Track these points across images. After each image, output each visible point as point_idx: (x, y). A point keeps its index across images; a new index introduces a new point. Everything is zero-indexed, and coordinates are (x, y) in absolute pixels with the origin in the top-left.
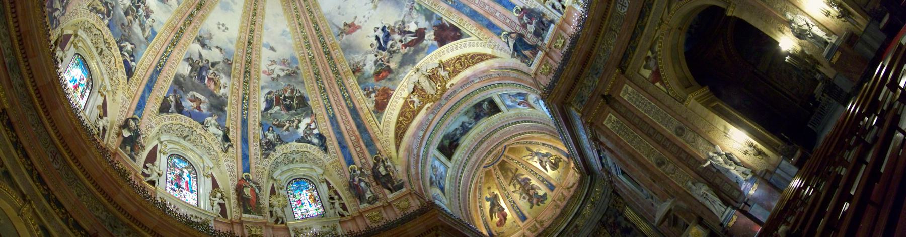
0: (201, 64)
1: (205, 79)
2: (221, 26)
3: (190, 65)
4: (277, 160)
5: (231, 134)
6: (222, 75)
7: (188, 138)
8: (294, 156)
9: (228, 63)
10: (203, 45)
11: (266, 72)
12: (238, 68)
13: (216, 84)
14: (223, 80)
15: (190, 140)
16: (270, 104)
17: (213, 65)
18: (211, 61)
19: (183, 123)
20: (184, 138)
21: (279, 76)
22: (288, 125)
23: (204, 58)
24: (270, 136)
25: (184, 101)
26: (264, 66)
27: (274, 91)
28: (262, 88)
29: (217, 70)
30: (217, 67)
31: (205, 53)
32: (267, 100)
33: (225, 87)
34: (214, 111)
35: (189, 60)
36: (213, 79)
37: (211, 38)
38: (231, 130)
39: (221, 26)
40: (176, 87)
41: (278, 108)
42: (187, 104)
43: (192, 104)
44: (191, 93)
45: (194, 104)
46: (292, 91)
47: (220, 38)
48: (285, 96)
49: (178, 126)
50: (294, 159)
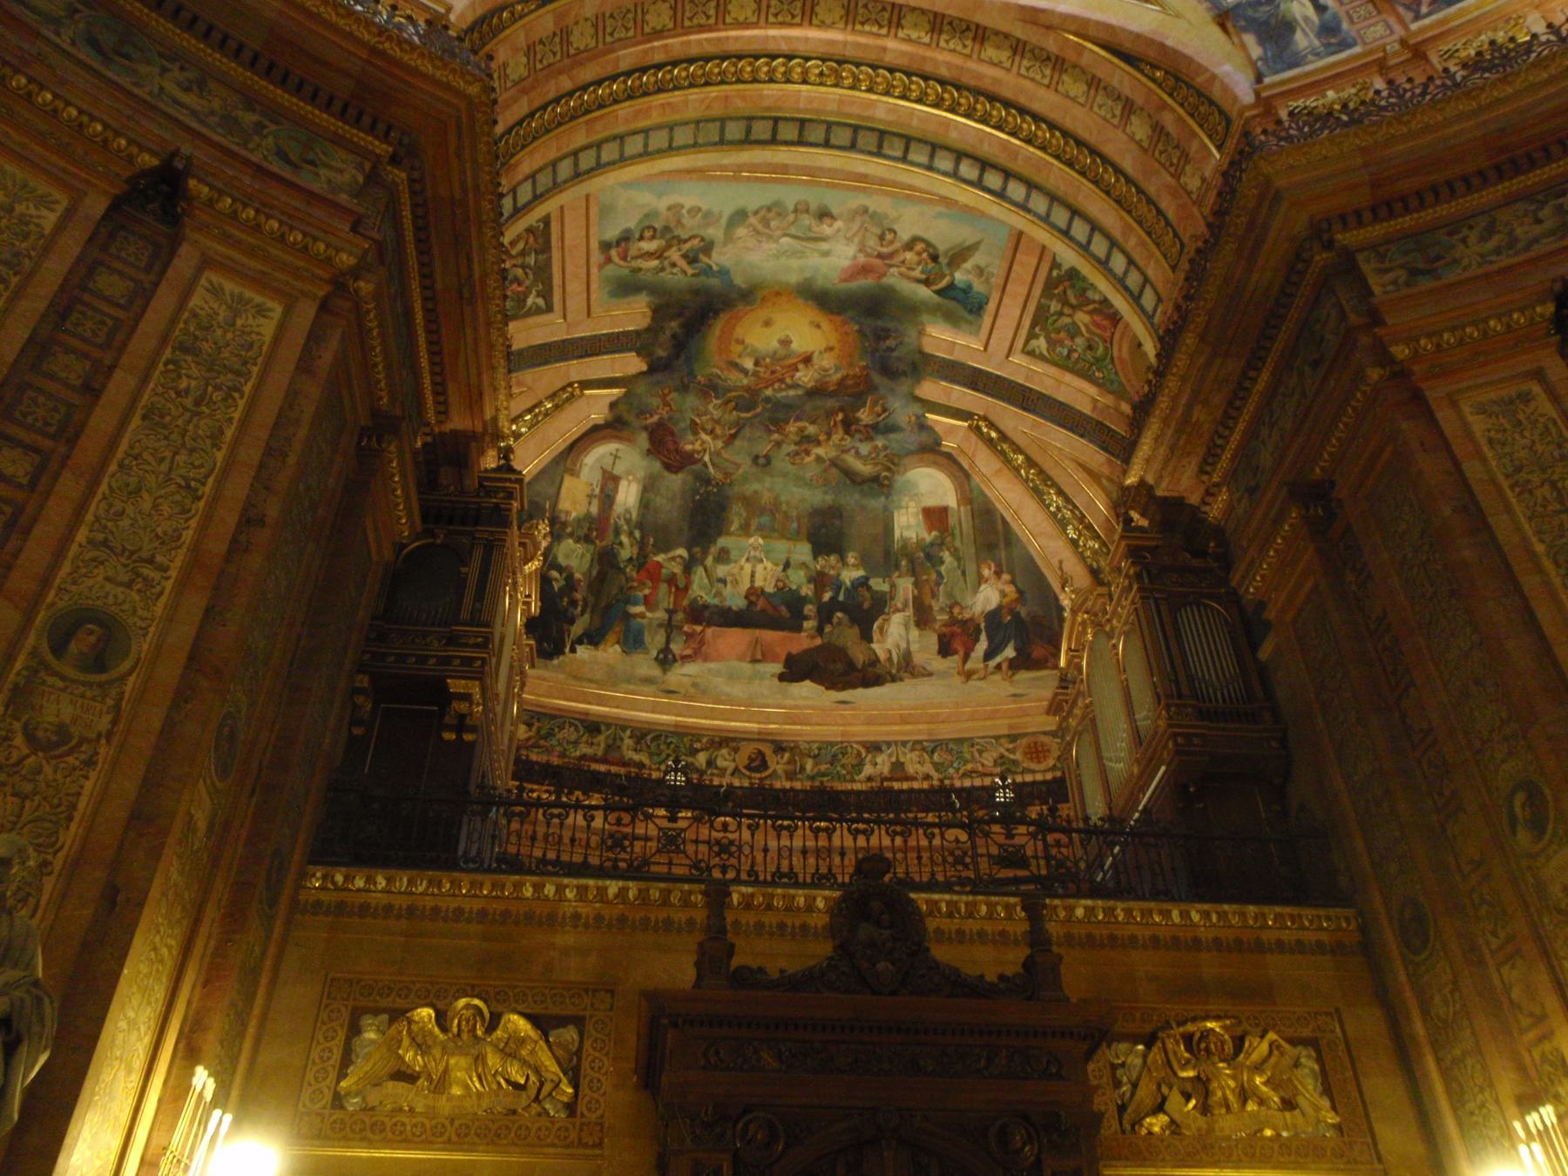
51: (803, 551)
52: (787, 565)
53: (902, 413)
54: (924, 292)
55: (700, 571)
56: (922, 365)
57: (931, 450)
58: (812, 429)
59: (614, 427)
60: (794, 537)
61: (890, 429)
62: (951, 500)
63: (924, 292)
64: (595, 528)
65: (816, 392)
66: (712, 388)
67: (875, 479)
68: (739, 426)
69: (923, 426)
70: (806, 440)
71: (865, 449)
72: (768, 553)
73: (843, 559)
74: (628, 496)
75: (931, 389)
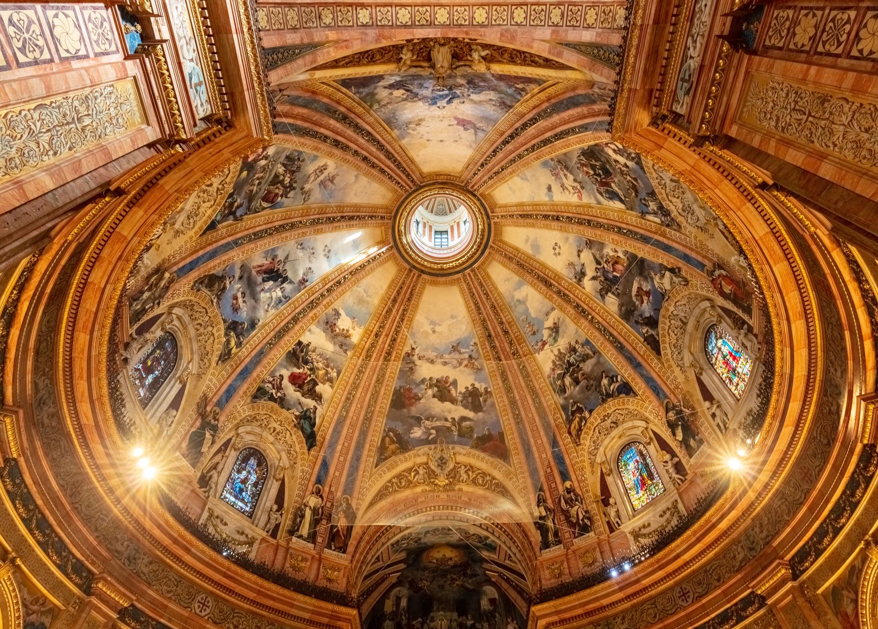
0: (602, 279)
1: (616, 277)
2: (557, 251)
3: (607, 293)
4: (680, 211)
5: (665, 263)
6: (605, 251)
7: (683, 319)
8: (668, 182)
9: (590, 244)
10: (583, 274)
11: (578, 196)
12: (590, 233)
13: (616, 263)
14: (608, 251)
15: (685, 317)
16: (613, 196)
17: (598, 263)
18: (594, 265)
19: (667, 328)
20: (685, 324)
21: (575, 180)
22: (629, 178)
23: (594, 274)
24: (653, 206)
25: (644, 312)
26: (574, 199)
27: (595, 187)
28: (599, 203)
29: (602, 258)
30: (598, 256)
31: (590, 272)
32: (611, 199)
33: (616, 251)
34: (646, 274)
35: (603, 293)
36: (613, 265)
37: (571, 264)
38: (660, 261)
39: (557, 251)
40: (633, 320)
41: (613, 185)
42: (646, 308)
43: (645, 302)
44: (634, 299)
45: (645, 298)
46: (583, 165)
47: (568, 252)
48: (595, 174)
49: (672, 334)
50: (672, 180)
51: (455, 615)
52: (451, 621)
53: (479, 571)
54: (479, 544)
55: (426, 626)
56: (483, 560)
57: (489, 581)
58: (454, 576)
59: (399, 583)
60: (452, 611)
61: (476, 575)
62: (497, 596)
63: (479, 544)
64: (395, 615)
65: (455, 566)
66: (425, 569)
67: (474, 590)
68: (434, 577)
69: (485, 575)
70: (453, 580)
71: (470, 581)
72: (445, 616)
73: (467, 617)
74: (404, 603)
75: (485, 565)
